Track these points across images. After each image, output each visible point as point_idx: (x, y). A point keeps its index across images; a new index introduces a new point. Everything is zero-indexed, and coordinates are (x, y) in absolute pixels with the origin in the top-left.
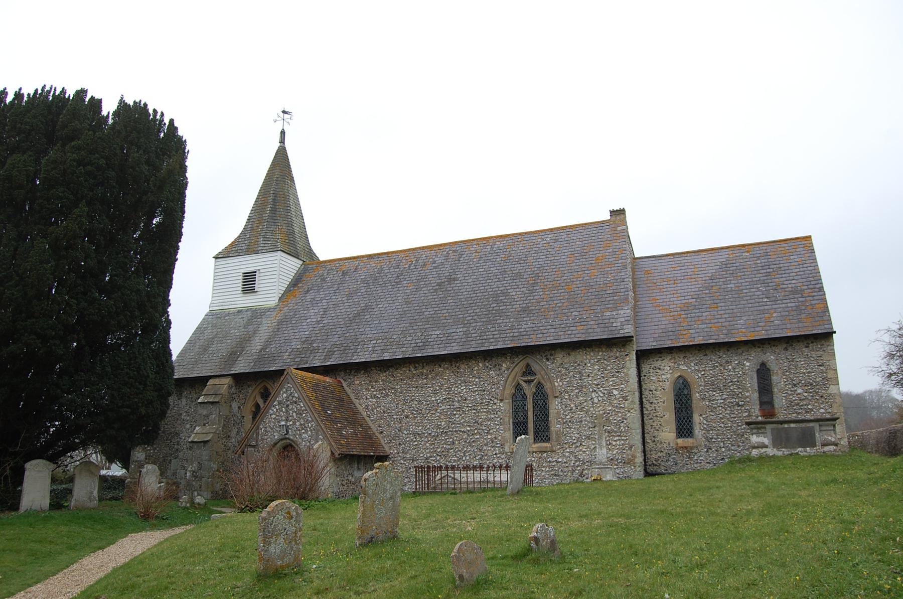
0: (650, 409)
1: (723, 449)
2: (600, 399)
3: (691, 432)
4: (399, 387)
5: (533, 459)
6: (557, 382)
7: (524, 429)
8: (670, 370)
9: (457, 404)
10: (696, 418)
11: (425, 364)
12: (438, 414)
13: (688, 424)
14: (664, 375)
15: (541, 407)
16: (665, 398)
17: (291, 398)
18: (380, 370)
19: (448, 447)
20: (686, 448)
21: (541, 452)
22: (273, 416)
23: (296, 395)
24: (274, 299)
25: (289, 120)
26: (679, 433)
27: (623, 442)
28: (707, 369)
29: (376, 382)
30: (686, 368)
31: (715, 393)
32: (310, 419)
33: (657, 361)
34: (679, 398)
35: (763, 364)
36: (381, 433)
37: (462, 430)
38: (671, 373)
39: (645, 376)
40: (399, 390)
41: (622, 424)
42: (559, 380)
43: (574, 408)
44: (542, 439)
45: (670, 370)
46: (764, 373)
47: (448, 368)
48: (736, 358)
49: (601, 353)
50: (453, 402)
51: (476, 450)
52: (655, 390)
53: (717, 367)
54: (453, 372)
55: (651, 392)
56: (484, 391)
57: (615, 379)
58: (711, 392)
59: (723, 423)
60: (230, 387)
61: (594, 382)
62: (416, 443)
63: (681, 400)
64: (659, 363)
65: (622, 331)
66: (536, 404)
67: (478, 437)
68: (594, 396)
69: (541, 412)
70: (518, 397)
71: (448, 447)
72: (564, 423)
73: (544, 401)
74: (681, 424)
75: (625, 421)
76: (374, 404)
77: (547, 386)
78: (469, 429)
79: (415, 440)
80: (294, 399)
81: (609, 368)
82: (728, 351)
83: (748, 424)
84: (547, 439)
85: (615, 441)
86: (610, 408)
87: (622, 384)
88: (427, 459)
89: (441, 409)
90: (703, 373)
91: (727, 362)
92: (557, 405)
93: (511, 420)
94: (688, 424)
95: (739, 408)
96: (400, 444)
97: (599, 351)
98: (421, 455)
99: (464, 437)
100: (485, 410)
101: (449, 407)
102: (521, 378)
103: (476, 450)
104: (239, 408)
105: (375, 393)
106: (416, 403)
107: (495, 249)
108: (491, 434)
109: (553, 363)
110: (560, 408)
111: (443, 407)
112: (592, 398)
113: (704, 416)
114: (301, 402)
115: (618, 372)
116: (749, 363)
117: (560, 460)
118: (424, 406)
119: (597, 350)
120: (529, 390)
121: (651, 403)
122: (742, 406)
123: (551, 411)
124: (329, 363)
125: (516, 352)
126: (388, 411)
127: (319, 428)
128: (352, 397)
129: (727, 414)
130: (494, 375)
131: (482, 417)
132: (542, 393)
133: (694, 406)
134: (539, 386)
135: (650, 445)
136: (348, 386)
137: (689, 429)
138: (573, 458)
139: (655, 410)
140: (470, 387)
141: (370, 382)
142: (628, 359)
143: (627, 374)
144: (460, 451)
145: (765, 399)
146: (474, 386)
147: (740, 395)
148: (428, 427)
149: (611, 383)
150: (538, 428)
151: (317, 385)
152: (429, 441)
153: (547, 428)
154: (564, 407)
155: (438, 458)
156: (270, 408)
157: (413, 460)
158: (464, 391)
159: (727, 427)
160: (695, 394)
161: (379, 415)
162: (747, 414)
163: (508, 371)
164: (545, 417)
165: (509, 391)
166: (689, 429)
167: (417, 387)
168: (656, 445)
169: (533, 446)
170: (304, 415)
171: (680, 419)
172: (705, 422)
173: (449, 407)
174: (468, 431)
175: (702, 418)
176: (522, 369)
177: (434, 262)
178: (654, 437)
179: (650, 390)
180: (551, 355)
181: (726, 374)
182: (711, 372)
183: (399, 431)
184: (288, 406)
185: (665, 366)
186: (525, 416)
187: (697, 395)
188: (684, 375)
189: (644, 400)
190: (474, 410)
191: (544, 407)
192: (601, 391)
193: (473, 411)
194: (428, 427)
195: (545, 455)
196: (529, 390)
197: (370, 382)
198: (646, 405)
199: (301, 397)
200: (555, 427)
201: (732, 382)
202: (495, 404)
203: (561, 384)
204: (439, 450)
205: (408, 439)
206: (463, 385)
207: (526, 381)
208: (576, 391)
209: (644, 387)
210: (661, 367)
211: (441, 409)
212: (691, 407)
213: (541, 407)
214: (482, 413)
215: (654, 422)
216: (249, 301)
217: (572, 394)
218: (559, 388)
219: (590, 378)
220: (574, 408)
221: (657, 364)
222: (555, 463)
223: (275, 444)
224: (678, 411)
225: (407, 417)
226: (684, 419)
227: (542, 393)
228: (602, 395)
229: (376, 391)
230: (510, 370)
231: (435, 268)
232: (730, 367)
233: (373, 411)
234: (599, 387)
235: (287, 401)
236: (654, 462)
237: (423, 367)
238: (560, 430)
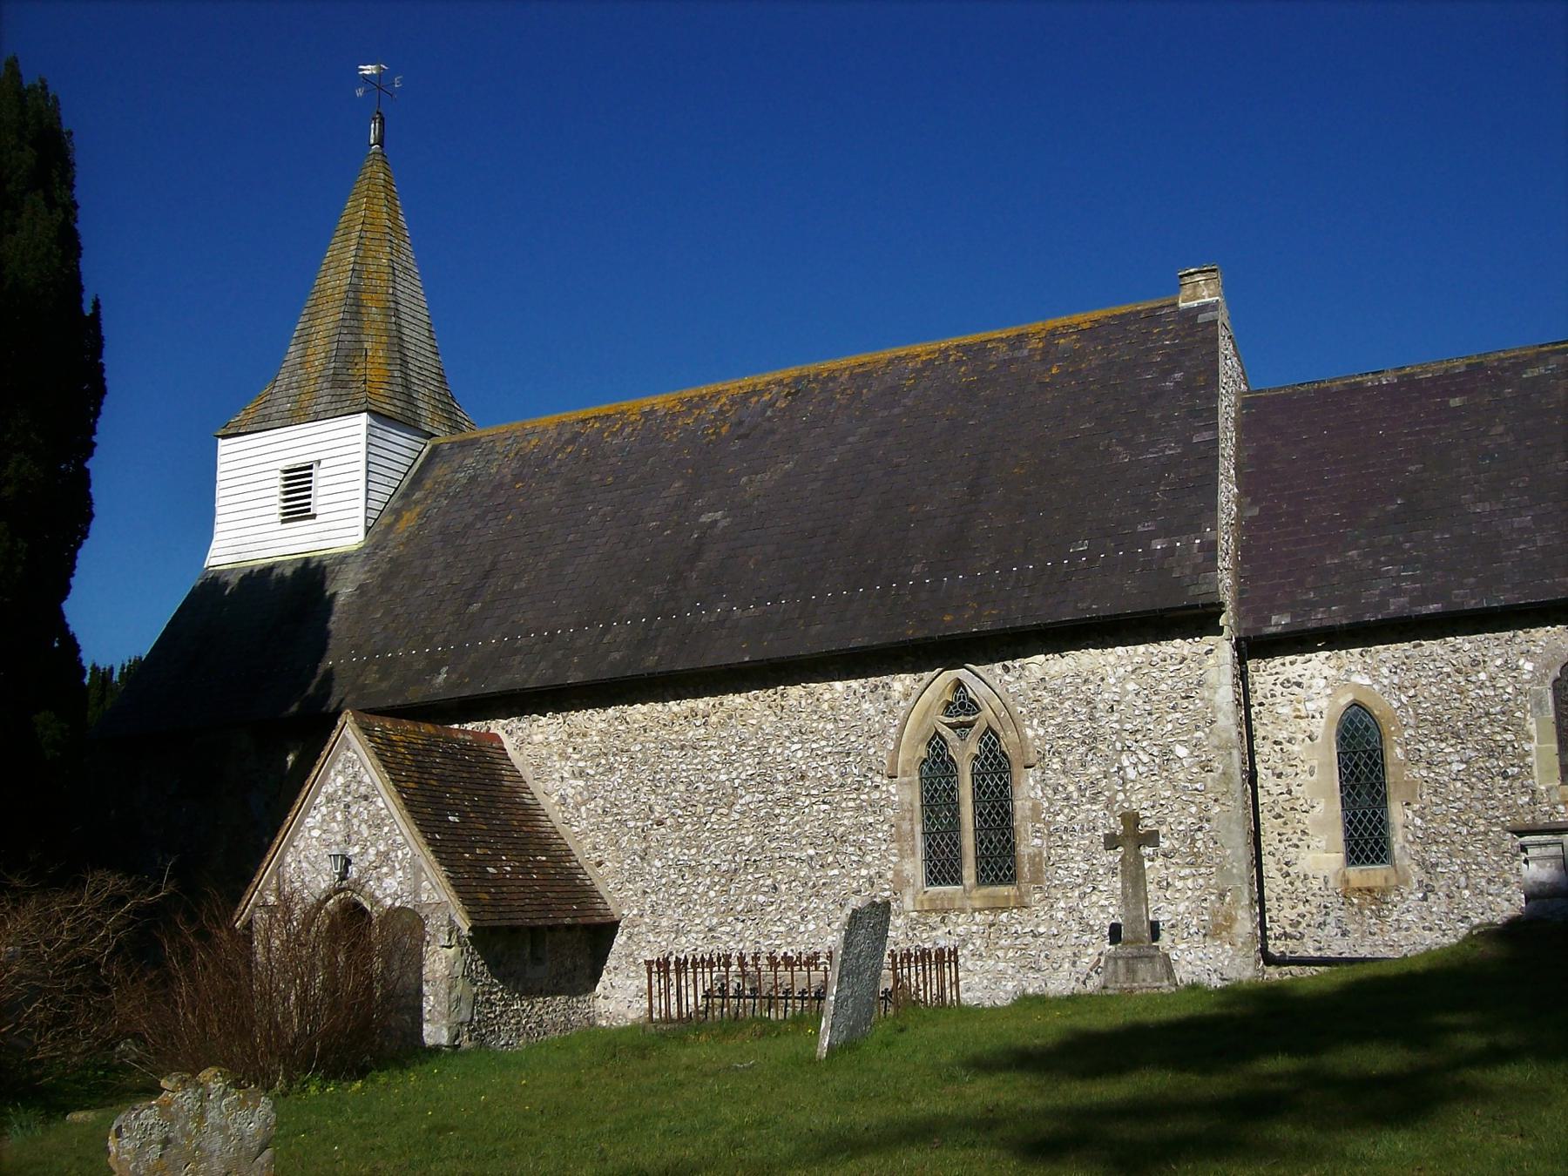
1: (1467, 893)
2: (1141, 769)
3: (1382, 850)
4: (638, 747)
5: (974, 928)
6: (1031, 727)
7: (951, 851)
8: (1326, 687)
9: (781, 788)
10: (1398, 813)
12: (737, 816)
13: (1375, 828)
14: (1310, 700)
15: (993, 792)
16: (1315, 763)
17: (354, 786)
19: (761, 899)
20: (1370, 890)
21: (993, 909)
22: (316, 833)
26: (1352, 851)
27: (1201, 881)
28: (1424, 681)
29: (585, 735)
30: (1367, 681)
31: (1443, 745)
34: (1351, 759)
36: (599, 864)
37: (797, 855)
38: (1329, 696)
39: (1261, 704)
40: (640, 755)
41: (1200, 835)
42: (1035, 722)
43: (1075, 795)
44: (997, 876)
45: (1326, 687)
48: (1497, 651)
51: (831, 907)
52: (1289, 742)
53: (1449, 676)
54: (770, 707)
55: (1277, 748)
56: (848, 754)
57: (1178, 715)
58: (1433, 744)
61: (1128, 726)
62: (683, 890)
63: (1356, 765)
65: (1193, 591)
66: (979, 787)
67: (836, 872)
68: (1126, 763)
69: (993, 807)
70: (937, 767)
71: (761, 899)
72: (1050, 835)
73: (1001, 778)
74: (1356, 829)
76: (581, 794)
77: (1008, 739)
79: (681, 881)
81: (1164, 687)
84: (1010, 878)
85: (1181, 878)
86: (1168, 794)
87: (1197, 728)
88: (710, 930)
89: (740, 802)
90: (1412, 693)
91: (1475, 663)
92: (1033, 788)
93: (918, 828)
94: (1375, 828)
95: (1507, 783)
96: (645, 892)
98: (698, 921)
99: (802, 874)
100: (851, 804)
101: (762, 797)
102: (948, 720)
103: (831, 907)
105: (581, 764)
108: (868, 866)
109: (1020, 677)
110: (1040, 794)
111: (748, 798)
112: (1120, 769)
113: (1416, 807)
114: (380, 795)
115: (1188, 697)
117: (1042, 930)
118: (702, 794)
122: (1515, 777)
123: (1018, 804)
126: (615, 810)
129: (1477, 799)
130: (872, 711)
131: (846, 822)
132: (995, 757)
133: (1390, 780)
137: (1377, 842)
138: (1075, 927)
139: (1289, 792)
140: (814, 746)
142: (1211, 662)
143: (1208, 703)
144: (791, 908)
146: (823, 743)
147: (1509, 749)
148: (713, 848)
149: (1170, 726)
150: (987, 848)
152: (716, 884)
153: (1009, 847)
154: (1050, 792)
155: (740, 926)
157: (677, 932)
158: (800, 754)
159: (1475, 835)
160: (1392, 748)
161: (592, 820)
163: (906, 700)
164: (1003, 820)
165: (913, 752)
166: (1377, 842)
167: (683, 747)
168: (1292, 884)
169: (975, 893)
170: (386, 829)
171: (1355, 815)
172: (1418, 822)
173: (762, 797)
174: (811, 858)
175: (1410, 813)
176: (941, 696)
178: (1287, 864)
179: (1276, 743)
181: (1473, 694)
182: (1434, 690)
183: (642, 859)
185: (1312, 677)
186: (953, 816)
187: (1398, 750)
188: (1364, 700)
189: (1260, 767)
190: (824, 803)
191: (1001, 792)
192: (1143, 749)
193: (826, 807)
194: (713, 848)
195: (1004, 916)
197: (570, 735)
200: (1029, 843)
201: (1487, 714)
202: (877, 787)
203: (1041, 732)
204: (739, 908)
205: (664, 881)
206: (796, 739)
208: (1083, 749)
209: (1260, 732)
210: (1303, 680)
211: (742, 801)
212: (1383, 784)
213: (993, 792)
214: (844, 810)
215: (1285, 823)
217: (1070, 758)
218: (1037, 742)
219: (1116, 716)
220: (1075, 795)
222: (1029, 938)
224: (1349, 795)
225: (660, 823)
226: (1364, 814)
227: (995, 757)
228: (1145, 759)
230: (912, 700)
232: (1482, 676)
233: (578, 810)
234: (1139, 737)
236: (1289, 929)
238: (1041, 854)
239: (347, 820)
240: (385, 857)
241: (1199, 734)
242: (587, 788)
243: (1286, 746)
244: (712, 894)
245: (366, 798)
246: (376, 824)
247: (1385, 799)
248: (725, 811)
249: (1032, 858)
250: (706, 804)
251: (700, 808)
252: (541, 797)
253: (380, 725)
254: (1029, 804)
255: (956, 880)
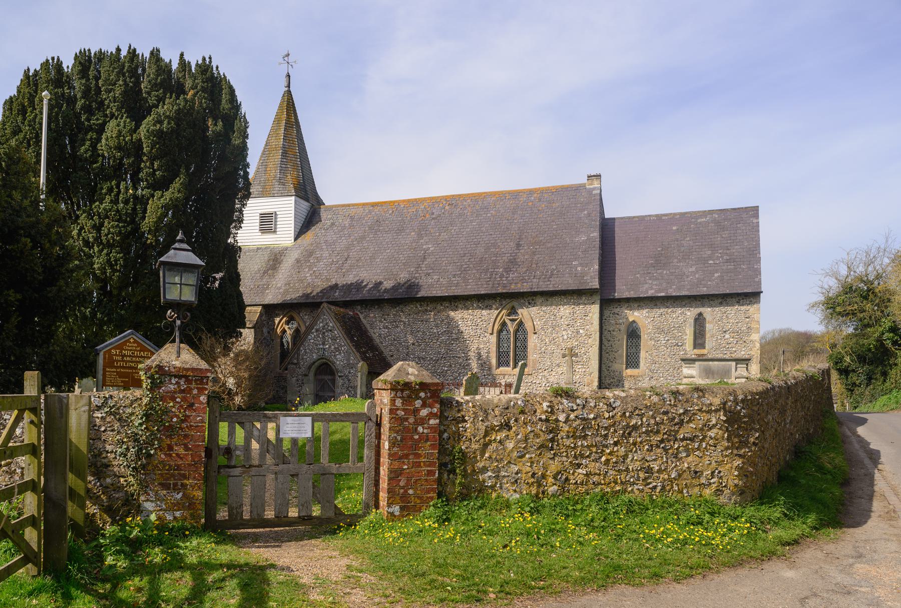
0: (607, 345)
1: (662, 379)
3: (638, 365)
11: (429, 303)
17: (326, 327)
18: (392, 306)
22: (312, 341)
23: (331, 325)
24: (290, 239)
25: (293, 64)
29: (388, 315)
32: (343, 344)
33: (616, 308)
35: (700, 314)
36: (392, 356)
37: (458, 356)
46: (699, 321)
47: (448, 307)
49: (572, 301)
50: (451, 334)
56: (477, 326)
59: (664, 358)
60: (261, 316)
64: (618, 309)
75: (588, 354)
77: (528, 325)
78: (463, 355)
80: (329, 328)
82: (674, 302)
83: (683, 360)
97: (571, 299)
104: (269, 332)
106: (421, 333)
107: (485, 205)
111: (443, 338)
116: (690, 313)
119: (569, 298)
120: (511, 327)
121: (609, 341)
124: (348, 299)
125: (504, 296)
127: (350, 351)
128: (368, 326)
134: (521, 324)
135: (605, 372)
136: (365, 318)
137: (636, 362)
141: (383, 315)
145: (700, 341)
151: (344, 317)
156: (309, 335)
162: (683, 353)
166: (636, 362)
167: (422, 321)
177: (433, 214)
180: (533, 300)
183: (407, 355)
184: (324, 333)
189: (603, 338)
196: (511, 327)
197: (383, 315)
198: (605, 342)
199: (335, 326)
207: (511, 320)
209: (604, 328)
216: (268, 240)
219: (562, 320)
221: (616, 311)
223: (314, 363)
229: (388, 323)
231: (433, 219)
234: (569, 326)
235: (323, 329)
237: (427, 305)
239: (323, 337)
240: (337, 349)
241: (588, 327)
242: (388, 332)
243: (612, 332)
244: (430, 366)
245: (331, 331)
246: (334, 339)
247: (640, 350)
248: (435, 341)
249: (533, 360)
250: (429, 339)
251: (427, 340)
252: (373, 335)
253: (333, 307)
254: (533, 344)
255: (508, 365)
